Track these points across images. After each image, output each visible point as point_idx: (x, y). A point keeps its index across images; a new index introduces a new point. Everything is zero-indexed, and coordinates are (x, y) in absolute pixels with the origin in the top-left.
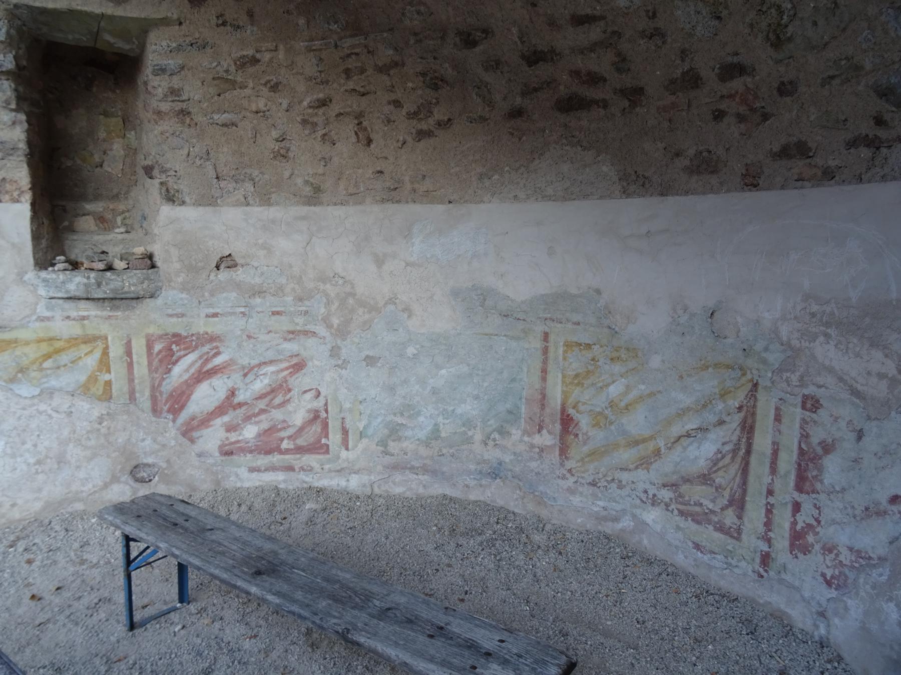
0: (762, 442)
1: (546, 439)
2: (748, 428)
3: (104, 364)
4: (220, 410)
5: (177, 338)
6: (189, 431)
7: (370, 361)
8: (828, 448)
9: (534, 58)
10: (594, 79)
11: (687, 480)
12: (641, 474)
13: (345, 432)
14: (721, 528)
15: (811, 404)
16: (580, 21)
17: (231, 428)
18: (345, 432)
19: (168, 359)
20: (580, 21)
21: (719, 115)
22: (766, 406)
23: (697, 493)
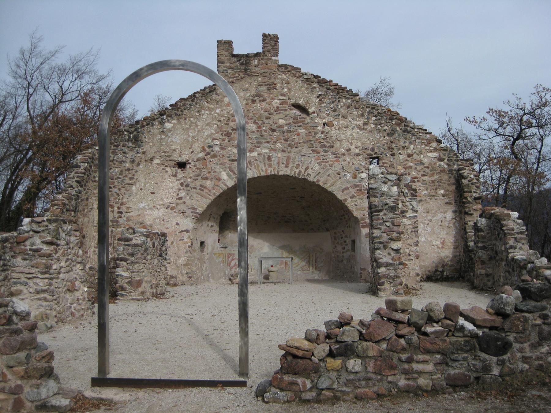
0: (311, 259)
1: (283, 266)
2: (310, 258)
3: (223, 258)
4: (234, 266)
5: (230, 254)
6: (231, 269)
7: (255, 257)
8: (318, 258)
9: (283, 216)
10: (290, 220)
11: (303, 266)
12: (297, 268)
13: (251, 269)
14: (308, 271)
15: (316, 254)
16: (289, 214)
17: (235, 269)
18: (251, 269)
19: (229, 257)
20: (289, 214)
21: (304, 225)
22: (311, 255)
23: (305, 268)
